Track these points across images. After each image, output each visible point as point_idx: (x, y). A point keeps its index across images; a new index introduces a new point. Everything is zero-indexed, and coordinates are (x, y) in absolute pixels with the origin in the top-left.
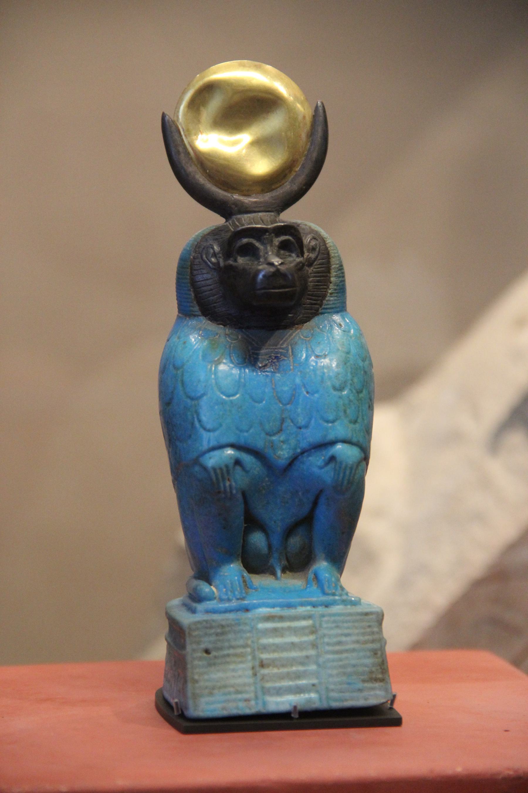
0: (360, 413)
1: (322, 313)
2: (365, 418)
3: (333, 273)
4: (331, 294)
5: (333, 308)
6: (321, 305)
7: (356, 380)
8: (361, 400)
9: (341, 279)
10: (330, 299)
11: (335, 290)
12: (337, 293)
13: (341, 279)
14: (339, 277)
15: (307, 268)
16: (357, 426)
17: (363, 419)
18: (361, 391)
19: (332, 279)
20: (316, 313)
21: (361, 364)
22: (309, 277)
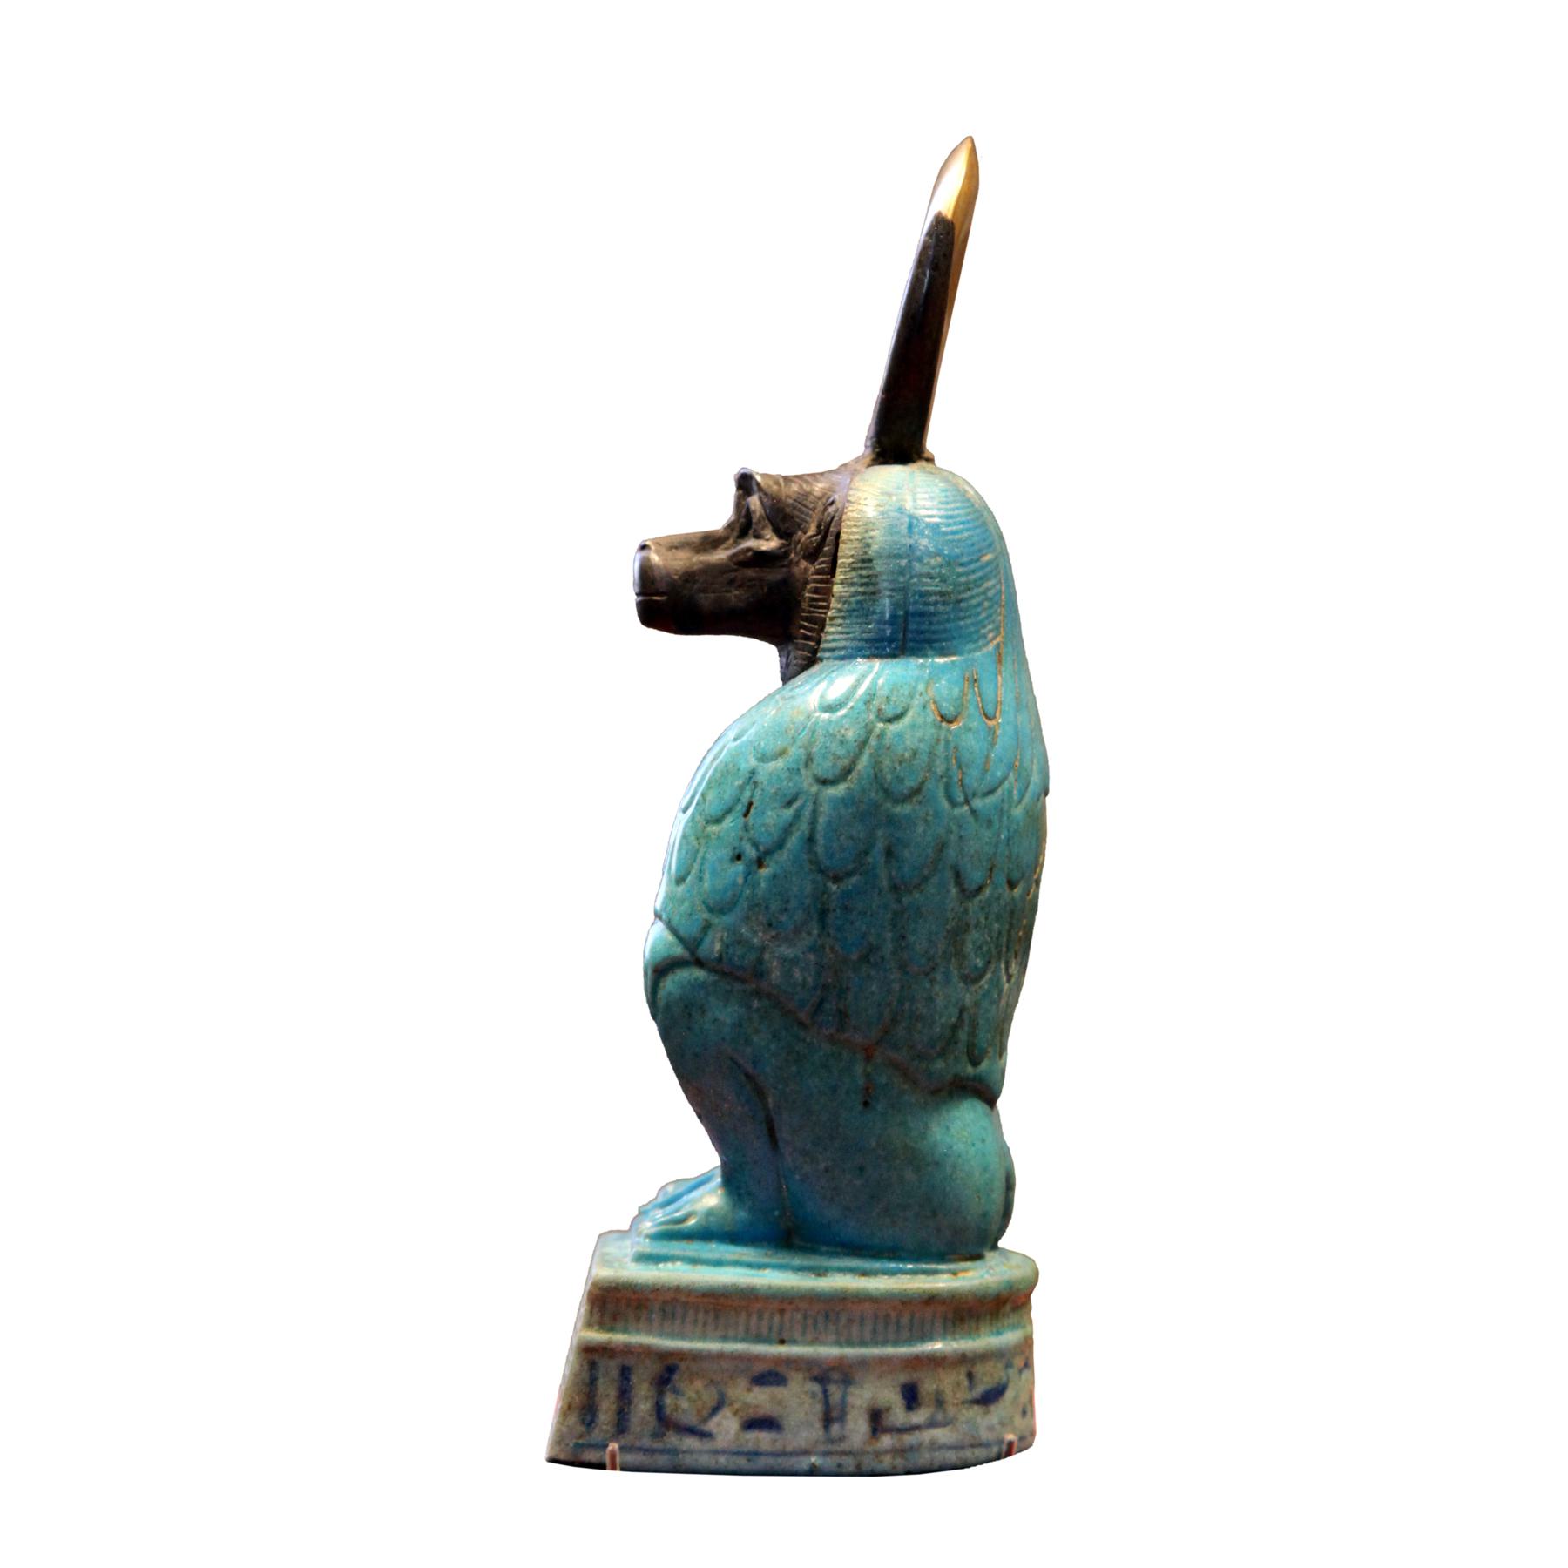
0: (696, 867)
1: (821, 660)
2: (707, 876)
3: (839, 576)
4: (832, 618)
5: (832, 650)
6: (819, 642)
7: (710, 796)
8: (708, 837)
9: (853, 589)
10: (833, 634)
11: (840, 610)
12: (844, 618)
13: (853, 589)
14: (853, 584)
15: (804, 564)
16: (681, 889)
17: (701, 879)
18: (718, 821)
19: (837, 588)
20: (811, 661)
21: (753, 762)
22: (806, 582)
